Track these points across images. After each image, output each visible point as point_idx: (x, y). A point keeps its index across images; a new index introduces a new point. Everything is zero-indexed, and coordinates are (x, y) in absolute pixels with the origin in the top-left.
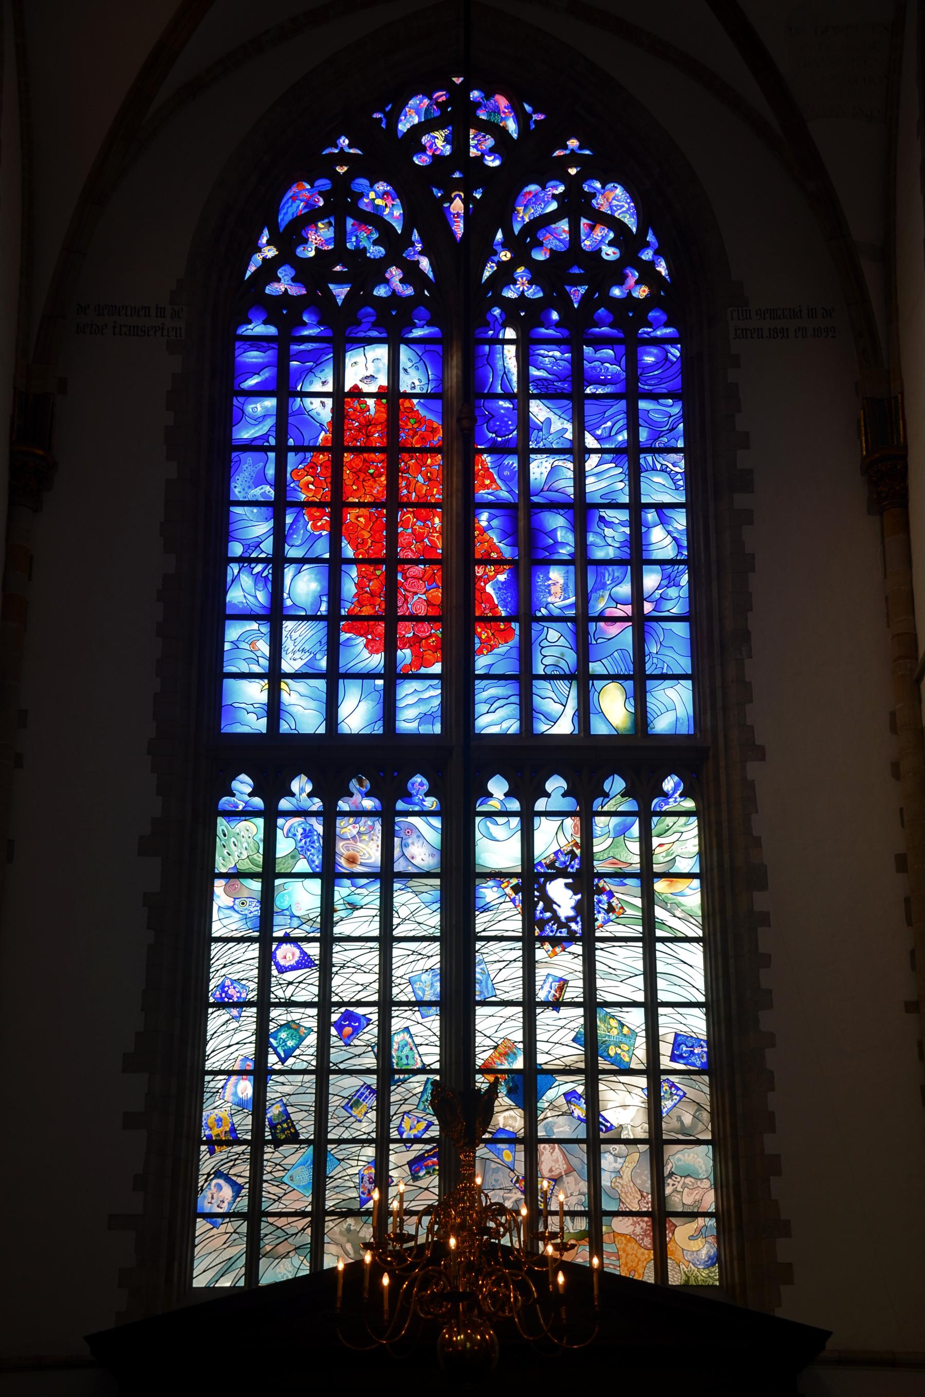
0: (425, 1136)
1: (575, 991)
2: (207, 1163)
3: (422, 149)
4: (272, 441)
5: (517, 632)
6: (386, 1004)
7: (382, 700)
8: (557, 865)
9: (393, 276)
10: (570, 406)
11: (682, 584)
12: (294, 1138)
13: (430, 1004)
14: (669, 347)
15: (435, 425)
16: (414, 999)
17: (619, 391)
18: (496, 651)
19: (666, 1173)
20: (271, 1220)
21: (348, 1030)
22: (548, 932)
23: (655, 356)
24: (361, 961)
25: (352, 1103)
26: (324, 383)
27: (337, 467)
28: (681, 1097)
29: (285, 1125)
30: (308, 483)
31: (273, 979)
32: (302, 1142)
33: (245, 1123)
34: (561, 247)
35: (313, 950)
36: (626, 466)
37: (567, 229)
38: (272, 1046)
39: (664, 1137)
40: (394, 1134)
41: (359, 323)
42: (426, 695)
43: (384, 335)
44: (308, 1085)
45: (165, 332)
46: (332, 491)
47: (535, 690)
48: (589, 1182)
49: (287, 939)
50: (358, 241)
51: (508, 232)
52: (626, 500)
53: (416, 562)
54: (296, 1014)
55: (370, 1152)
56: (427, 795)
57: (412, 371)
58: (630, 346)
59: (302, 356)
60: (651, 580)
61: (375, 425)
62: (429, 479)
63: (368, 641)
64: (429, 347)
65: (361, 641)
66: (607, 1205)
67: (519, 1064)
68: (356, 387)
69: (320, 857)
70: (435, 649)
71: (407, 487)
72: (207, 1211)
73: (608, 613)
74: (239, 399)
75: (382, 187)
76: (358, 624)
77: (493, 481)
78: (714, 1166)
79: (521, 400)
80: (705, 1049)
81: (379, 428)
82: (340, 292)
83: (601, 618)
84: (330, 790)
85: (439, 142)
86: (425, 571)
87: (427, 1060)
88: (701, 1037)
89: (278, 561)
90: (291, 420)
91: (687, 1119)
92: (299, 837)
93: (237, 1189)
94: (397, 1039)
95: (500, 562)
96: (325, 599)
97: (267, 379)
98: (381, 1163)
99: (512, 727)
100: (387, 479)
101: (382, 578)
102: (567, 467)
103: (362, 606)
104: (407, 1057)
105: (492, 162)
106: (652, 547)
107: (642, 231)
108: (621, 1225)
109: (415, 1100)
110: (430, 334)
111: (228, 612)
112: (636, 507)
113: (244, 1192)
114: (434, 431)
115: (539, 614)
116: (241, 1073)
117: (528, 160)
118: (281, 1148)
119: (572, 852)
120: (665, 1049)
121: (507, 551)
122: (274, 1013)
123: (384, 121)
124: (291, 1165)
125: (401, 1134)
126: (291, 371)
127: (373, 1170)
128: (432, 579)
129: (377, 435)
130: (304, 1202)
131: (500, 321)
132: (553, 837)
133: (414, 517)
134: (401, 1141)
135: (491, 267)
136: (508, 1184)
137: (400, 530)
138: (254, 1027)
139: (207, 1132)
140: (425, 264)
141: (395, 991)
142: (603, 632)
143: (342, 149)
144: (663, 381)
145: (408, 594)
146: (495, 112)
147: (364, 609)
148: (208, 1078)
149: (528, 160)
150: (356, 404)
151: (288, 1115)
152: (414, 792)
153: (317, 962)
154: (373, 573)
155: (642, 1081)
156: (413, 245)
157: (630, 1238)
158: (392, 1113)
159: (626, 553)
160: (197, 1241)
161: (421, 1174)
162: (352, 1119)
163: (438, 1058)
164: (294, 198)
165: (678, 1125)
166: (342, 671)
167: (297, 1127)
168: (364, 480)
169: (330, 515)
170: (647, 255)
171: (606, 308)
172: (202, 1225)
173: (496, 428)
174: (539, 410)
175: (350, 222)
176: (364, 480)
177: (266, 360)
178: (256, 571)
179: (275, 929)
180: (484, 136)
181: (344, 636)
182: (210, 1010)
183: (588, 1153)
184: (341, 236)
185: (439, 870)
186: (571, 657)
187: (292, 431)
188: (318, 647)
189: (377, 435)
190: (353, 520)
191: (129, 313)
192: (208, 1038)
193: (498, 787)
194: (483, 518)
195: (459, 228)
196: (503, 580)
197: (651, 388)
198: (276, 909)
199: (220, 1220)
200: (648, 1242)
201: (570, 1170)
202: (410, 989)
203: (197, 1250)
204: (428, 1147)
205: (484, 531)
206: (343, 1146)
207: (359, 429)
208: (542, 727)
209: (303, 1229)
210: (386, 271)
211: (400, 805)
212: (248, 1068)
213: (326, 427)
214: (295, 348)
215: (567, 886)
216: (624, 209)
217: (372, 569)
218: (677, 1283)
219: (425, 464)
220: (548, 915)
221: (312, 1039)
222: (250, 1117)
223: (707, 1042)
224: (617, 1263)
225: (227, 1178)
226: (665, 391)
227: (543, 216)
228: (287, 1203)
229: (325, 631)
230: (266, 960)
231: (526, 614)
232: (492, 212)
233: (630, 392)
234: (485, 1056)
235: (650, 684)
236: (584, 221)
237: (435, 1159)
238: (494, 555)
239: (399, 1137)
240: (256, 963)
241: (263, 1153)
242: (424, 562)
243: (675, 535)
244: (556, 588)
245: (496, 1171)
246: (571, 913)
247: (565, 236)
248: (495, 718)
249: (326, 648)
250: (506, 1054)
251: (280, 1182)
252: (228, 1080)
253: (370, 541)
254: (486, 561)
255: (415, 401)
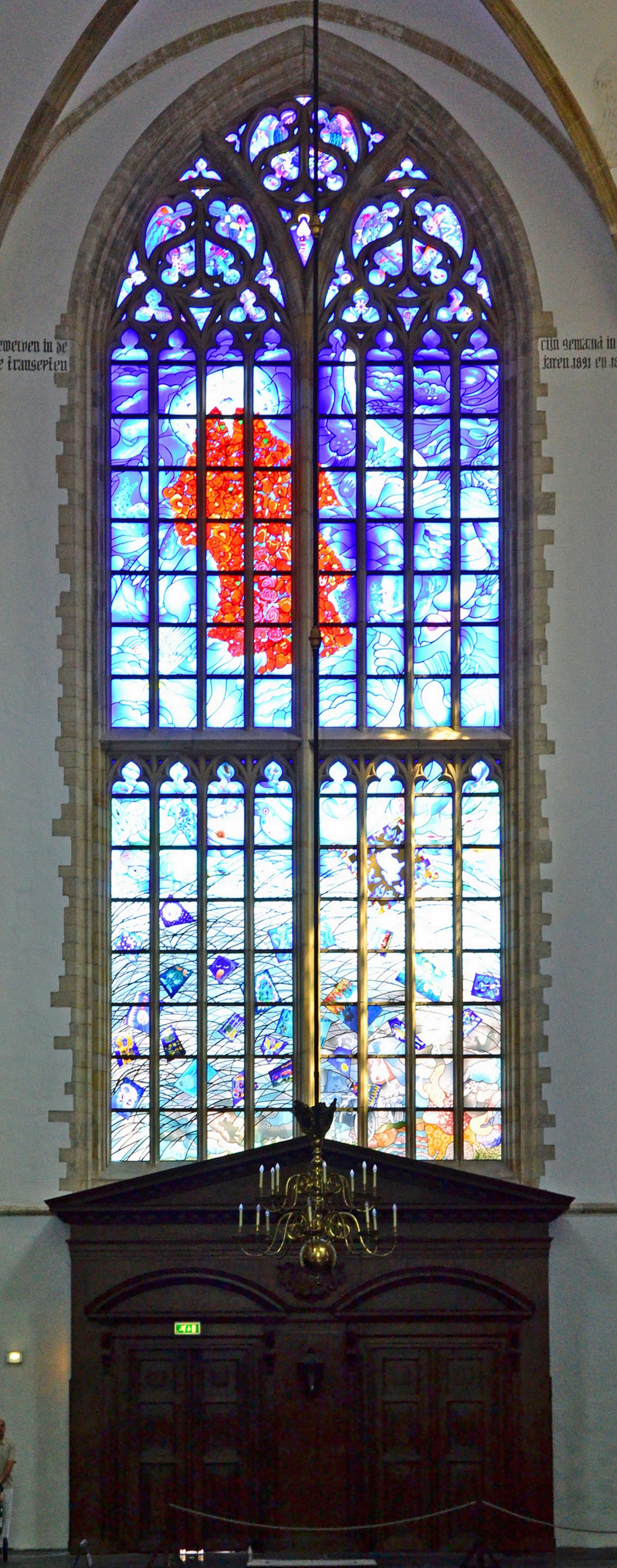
0: (282, 1053)
1: (398, 942)
2: (117, 1072)
3: (272, 172)
4: (146, 462)
5: (355, 637)
6: (249, 952)
7: (243, 698)
8: (386, 838)
9: (246, 300)
10: (402, 425)
11: (493, 593)
12: (182, 1054)
13: (284, 951)
14: (487, 368)
15: (285, 446)
16: (271, 948)
17: (444, 411)
18: (336, 653)
19: (465, 1079)
20: (167, 1114)
21: (221, 972)
22: (377, 894)
23: (476, 377)
24: (229, 917)
25: (225, 1029)
26: (188, 405)
27: (200, 486)
28: (479, 1022)
29: (175, 1045)
30: (177, 501)
31: (161, 932)
32: (188, 1057)
33: (144, 1043)
34: (395, 271)
35: (192, 908)
36: (449, 483)
37: (401, 252)
38: (162, 984)
39: (465, 1053)
40: (258, 1052)
41: (218, 346)
42: (278, 693)
43: (240, 358)
44: (191, 1014)
45: (53, 366)
46: (197, 508)
47: (368, 689)
48: (406, 1086)
49: (171, 900)
50: (216, 265)
51: (349, 257)
52: (447, 514)
53: (270, 573)
54: (179, 959)
55: (240, 1065)
56: (280, 779)
57: (265, 392)
58: (455, 366)
59: (169, 380)
60: (468, 584)
61: (233, 445)
62: (280, 497)
63: (231, 646)
64: (280, 369)
65: (225, 645)
66: (420, 1103)
67: (353, 999)
68: (216, 409)
69: (196, 832)
70: (286, 652)
71: (262, 503)
72: (119, 1107)
73: (430, 620)
74: (116, 420)
75: (236, 210)
76: (221, 630)
77: (335, 498)
78: (502, 1074)
79: (359, 419)
80: (499, 986)
81: (237, 448)
82: (201, 315)
83: (424, 624)
84: (202, 776)
85: (285, 164)
86: (277, 582)
87: (283, 995)
88: (495, 976)
89: (153, 573)
90: (161, 441)
91: (483, 1041)
92: (178, 815)
93: (141, 1091)
94: (259, 980)
95: (341, 573)
96: (194, 607)
97: (139, 402)
98: (248, 1072)
99: (352, 721)
100: (244, 497)
101: (241, 588)
102: (397, 481)
103: (224, 614)
104: (267, 993)
105: (335, 184)
106: (467, 559)
107: (467, 255)
108: (430, 1118)
109: (274, 1026)
110: (280, 356)
111: (114, 620)
112: (456, 521)
113: (146, 1093)
114: (283, 450)
115: (373, 621)
116: (139, 1005)
117: (366, 181)
118: (172, 1062)
119: (397, 828)
120: (467, 986)
121: (347, 564)
122: (163, 958)
123: (238, 143)
124: (180, 1074)
125: (263, 1051)
126: (160, 394)
127: (243, 1079)
128: (283, 589)
129: (234, 455)
130: (192, 1102)
131: (342, 344)
132: (383, 815)
133: (268, 532)
134: (263, 1056)
135: (333, 290)
136: (345, 1088)
137: (256, 544)
138: (148, 969)
139: (116, 1049)
140: (275, 288)
141: (257, 941)
142: (426, 636)
143: (200, 173)
144: (483, 401)
145: (263, 603)
146: (337, 133)
147: (226, 616)
148: (114, 1008)
149: (366, 181)
150: (216, 425)
151: (177, 1037)
152: (270, 777)
153: (195, 918)
154: (234, 584)
155: (450, 1010)
156: (264, 268)
157: (436, 1127)
158: (256, 1036)
159: (445, 565)
160: (113, 1128)
161: (279, 1081)
162: (226, 1040)
163: (291, 993)
164: (159, 223)
165: (475, 1044)
166: (209, 672)
167: (184, 1046)
168: (224, 498)
169: (196, 530)
170: (470, 278)
171: (434, 330)
172: (116, 1117)
173: (337, 448)
174: (374, 430)
175: (208, 245)
176: (224, 498)
177: (138, 384)
178: (135, 583)
179: (161, 891)
180: (327, 158)
181: (210, 641)
182: (114, 956)
183: (406, 1065)
184: (200, 261)
185: (290, 843)
186: (400, 659)
187: (162, 451)
188: (189, 651)
189: (234, 455)
190: (216, 535)
191: (21, 348)
192: (113, 977)
193: (338, 771)
194: (326, 532)
195: (305, 251)
196: (343, 590)
197: (471, 408)
198: (161, 875)
199: (129, 1114)
200: (450, 1129)
201: (392, 1077)
202: (268, 939)
203: (113, 1135)
204: (284, 1061)
205: (326, 545)
206: (219, 1060)
207: (219, 450)
208: (373, 720)
209: (191, 1121)
210: (240, 296)
211: (259, 789)
212: (145, 1001)
213: (191, 448)
214: (163, 372)
215: (394, 855)
216: (451, 232)
217: (232, 580)
218: (470, 1158)
219: (276, 482)
220: (378, 879)
221: (193, 979)
222: (148, 1038)
223: (501, 980)
224: (426, 1145)
225: (133, 1083)
226: (484, 411)
227: (378, 240)
228: (179, 1102)
229: (195, 637)
230: (155, 915)
231: (361, 620)
232: (334, 236)
233: (454, 414)
234: (328, 992)
235: (464, 682)
236: (416, 244)
237: (290, 1070)
238: (335, 567)
239: (261, 1054)
240: (147, 919)
241: (159, 1065)
242: (277, 573)
243: (489, 547)
244: (386, 598)
245: (336, 1079)
246: (397, 878)
247: (399, 259)
248: (336, 711)
249: (195, 651)
250: (343, 990)
251: (172, 1087)
252: (130, 1010)
253: (230, 554)
254: (329, 572)
255: (267, 422)
